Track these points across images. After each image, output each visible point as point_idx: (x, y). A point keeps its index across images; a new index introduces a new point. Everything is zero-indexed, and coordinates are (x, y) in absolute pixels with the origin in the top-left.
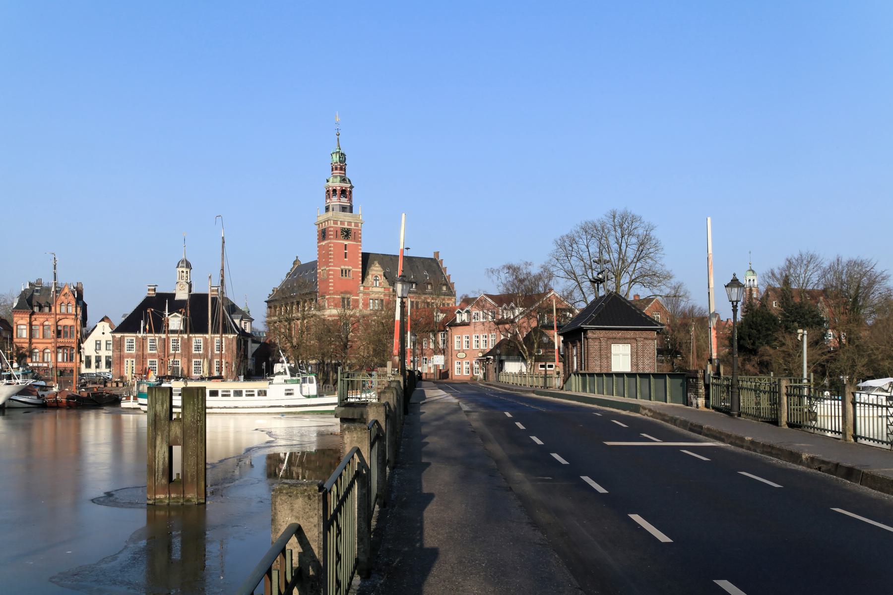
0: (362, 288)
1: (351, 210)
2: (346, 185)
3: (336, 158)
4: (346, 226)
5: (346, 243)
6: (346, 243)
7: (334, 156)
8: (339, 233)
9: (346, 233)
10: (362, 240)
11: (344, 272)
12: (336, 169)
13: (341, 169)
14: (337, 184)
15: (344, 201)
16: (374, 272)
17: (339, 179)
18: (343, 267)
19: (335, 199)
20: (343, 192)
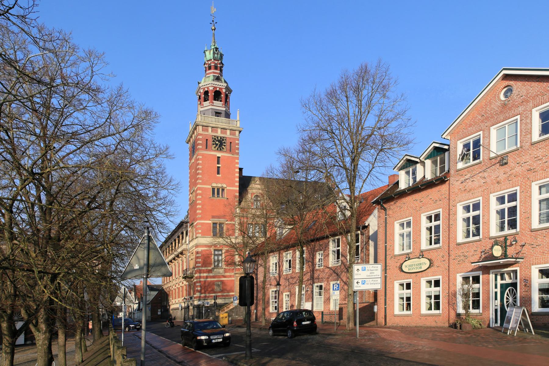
0: (238, 210)
1: (228, 115)
2: (221, 85)
3: (209, 55)
4: (219, 134)
5: (219, 154)
6: (219, 154)
7: (207, 53)
8: (210, 142)
9: (220, 143)
10: (240, 151)
11: (217, 192)
12: (210, 68)
13: (216, 68)
14: (208, 82)
15: (219, 105)
16: (254, 191)
17: (212, 78)
18: (214, 185)
19: (207, 103)
20: (217, 95)
